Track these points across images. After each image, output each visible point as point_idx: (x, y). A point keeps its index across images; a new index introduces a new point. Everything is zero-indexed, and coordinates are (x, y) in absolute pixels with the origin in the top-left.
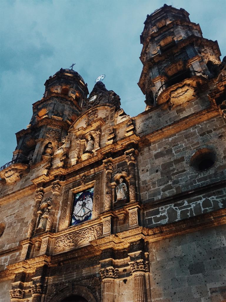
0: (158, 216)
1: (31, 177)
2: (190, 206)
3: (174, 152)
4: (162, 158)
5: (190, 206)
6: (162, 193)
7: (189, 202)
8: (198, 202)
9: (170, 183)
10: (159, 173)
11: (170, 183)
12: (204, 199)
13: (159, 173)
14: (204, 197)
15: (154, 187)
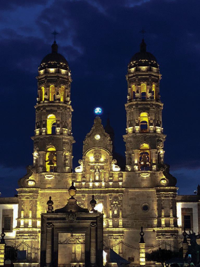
0: (128, 223)
1: (62, 180)
2: (138, 223)
3: (137, 200)
4: (132, 201)
5: (138, 223)
6: (130, 215)
7: (138, 221)
8: (141, 223)
9: (133, 213)
10: (130, 207)
11: (133, 213)
12: (142, 222)
13: (130, 207)
14: (143, 221)
15: (128, 212)
